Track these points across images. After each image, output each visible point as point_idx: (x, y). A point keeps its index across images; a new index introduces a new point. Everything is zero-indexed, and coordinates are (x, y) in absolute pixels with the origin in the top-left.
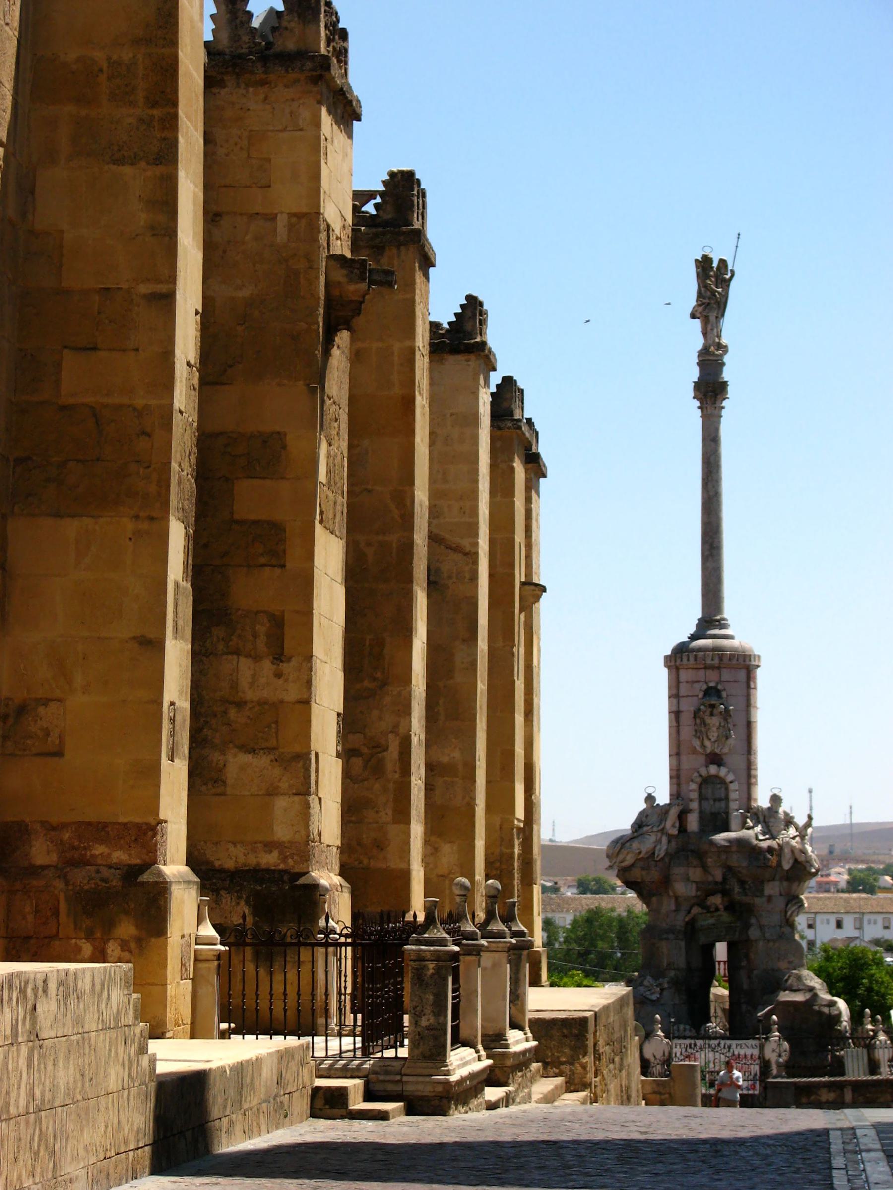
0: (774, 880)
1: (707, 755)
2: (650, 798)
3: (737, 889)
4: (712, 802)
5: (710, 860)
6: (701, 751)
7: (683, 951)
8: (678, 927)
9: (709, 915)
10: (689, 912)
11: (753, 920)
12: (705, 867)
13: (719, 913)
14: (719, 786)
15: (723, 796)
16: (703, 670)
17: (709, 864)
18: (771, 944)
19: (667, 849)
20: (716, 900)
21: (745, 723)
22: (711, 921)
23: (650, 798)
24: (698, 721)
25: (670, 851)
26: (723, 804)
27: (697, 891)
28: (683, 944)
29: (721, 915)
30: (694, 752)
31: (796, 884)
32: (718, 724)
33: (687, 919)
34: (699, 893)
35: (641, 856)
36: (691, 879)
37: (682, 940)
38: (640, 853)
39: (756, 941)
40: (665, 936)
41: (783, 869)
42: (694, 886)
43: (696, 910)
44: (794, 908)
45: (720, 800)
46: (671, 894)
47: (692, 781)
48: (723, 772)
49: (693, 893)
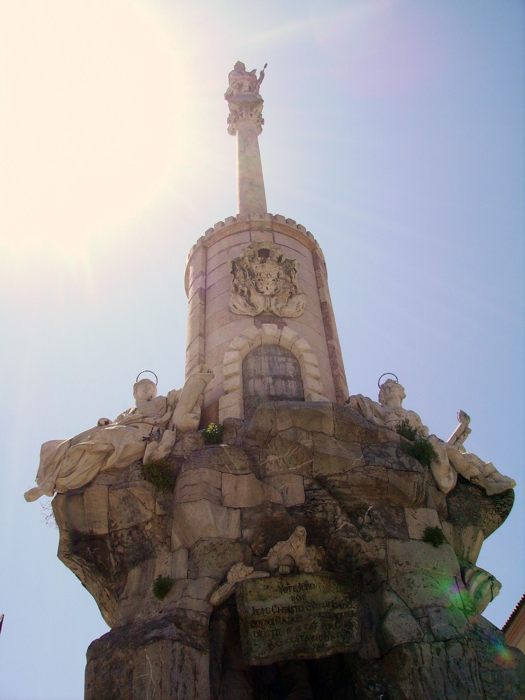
0: (425, 504)
1: (257, 316)
2: (144, 388)
3: (342, 521)
4: (270, 380)
5: (271, 458)
6: (248, 311)
7: (204, 682)
8: (191, 615)
9: (275, 583)
10: (223, 580)
11: (390, 598)
12: (261, 476)
13: (302, 579)
14: (284, 359)
15: (291, 373)
16: (247, 234)
17: (272, 468)
18: (456, 649)
19: (172, 448)
20: (295, 547)
21: (319, 306)
22: (285, 599)
23: (144, 388)
24: (240, 273)
25: (179, 452)
26: (292, 385)
27: (242, 528)
28: (203, 662)
29: (308, 586)
30: (233, 315)
31: (470, 530)
32: (274, 275)
33: (216, 598)
34: (247, 533)
35: (111, 461)
36: (228, 501)
37: (200, 649)
38: (108, 454)
39: (410, 645)
40: (153, 634)
41: (438, 488)
42: (236, 516)
43: (239, 573)
44: (481, 578)
45: (286, 378)
46: (177, 541)
47: (230, 350)
48: (288, 333)
49: (233, 532)
